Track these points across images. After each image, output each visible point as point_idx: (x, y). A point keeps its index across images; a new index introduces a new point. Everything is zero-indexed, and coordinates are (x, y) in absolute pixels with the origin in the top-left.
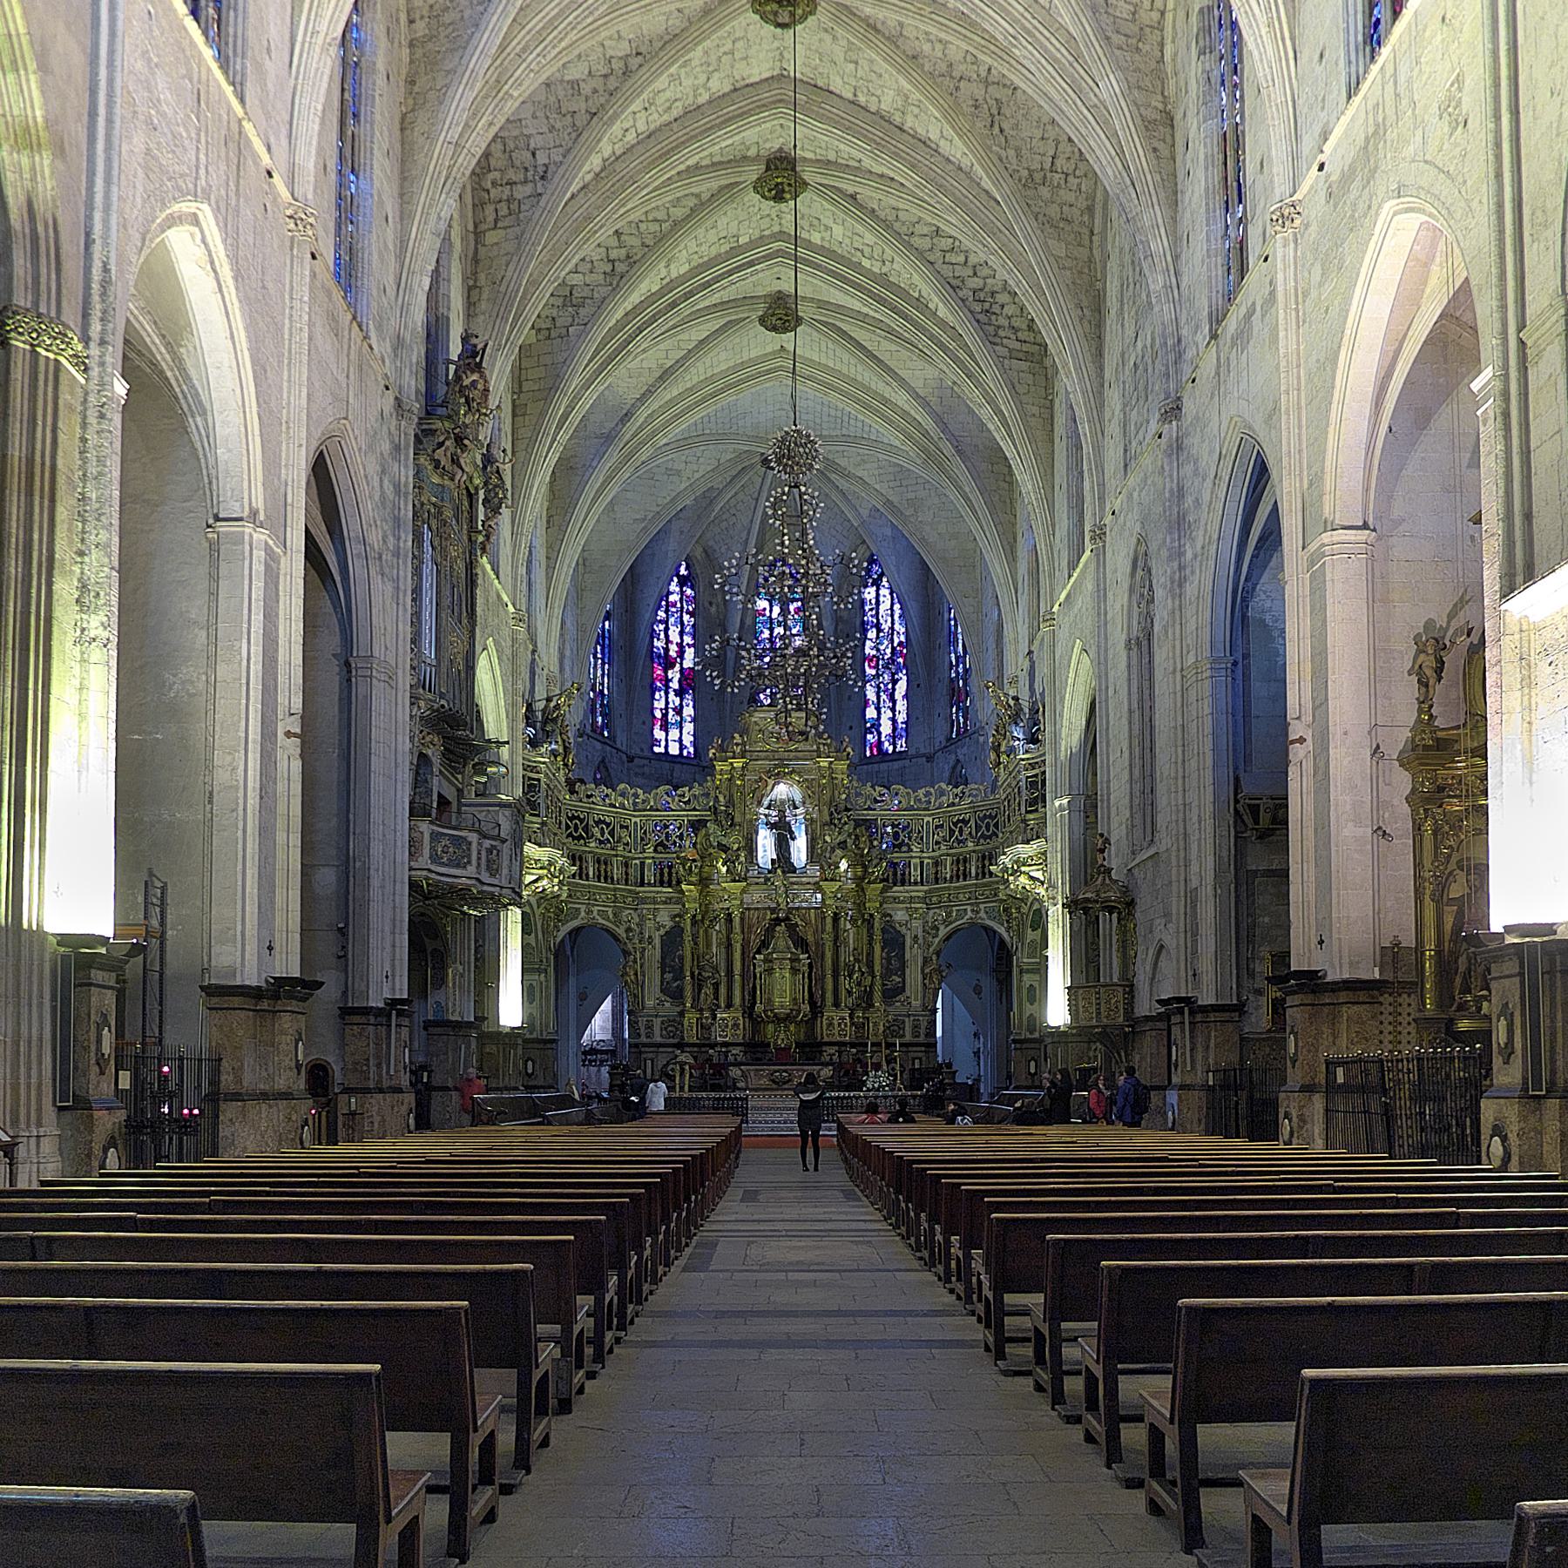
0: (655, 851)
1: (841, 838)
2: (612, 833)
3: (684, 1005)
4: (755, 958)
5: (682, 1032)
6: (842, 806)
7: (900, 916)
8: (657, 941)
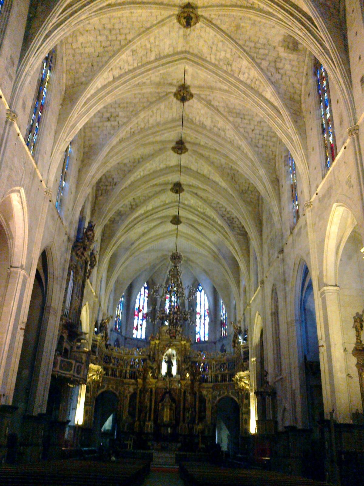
0: (130, 368)
1: (187, 367)
6: (188, 356)
7: (205, 393)
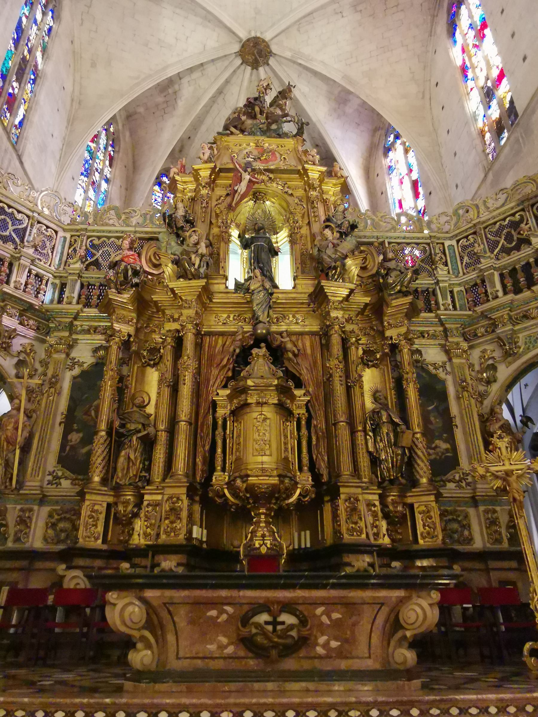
2: (22, 233)
3: (89, 480)
4: (218, 394)
5: (77, 530)
8: (66, 385)
